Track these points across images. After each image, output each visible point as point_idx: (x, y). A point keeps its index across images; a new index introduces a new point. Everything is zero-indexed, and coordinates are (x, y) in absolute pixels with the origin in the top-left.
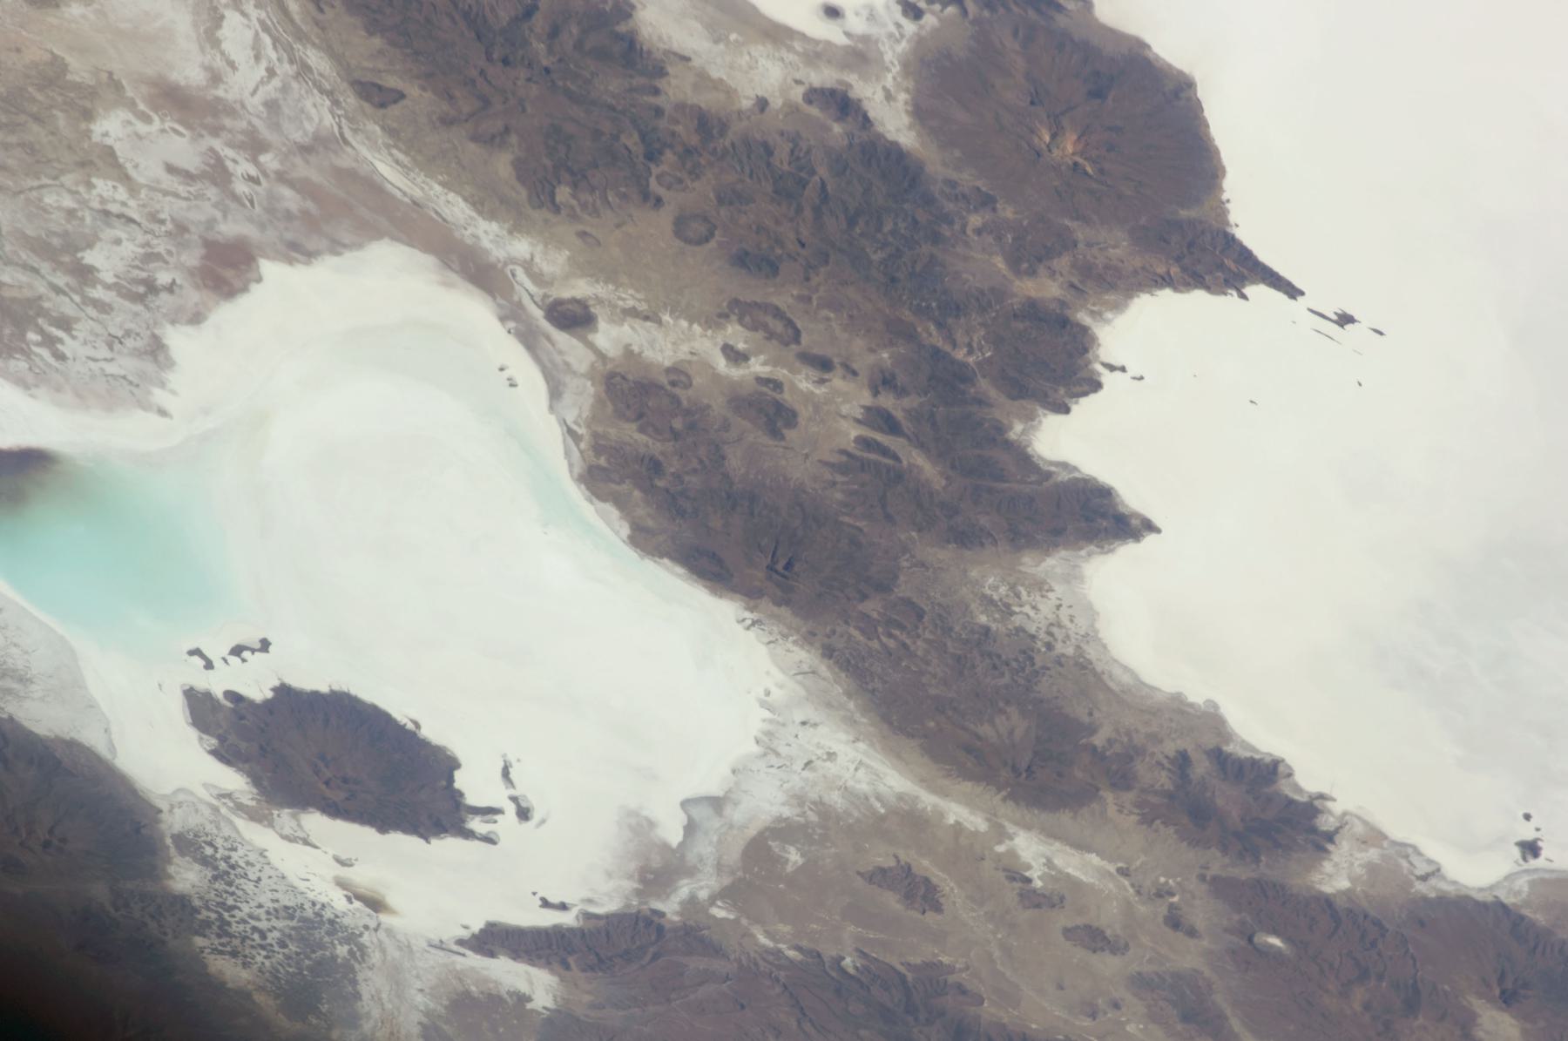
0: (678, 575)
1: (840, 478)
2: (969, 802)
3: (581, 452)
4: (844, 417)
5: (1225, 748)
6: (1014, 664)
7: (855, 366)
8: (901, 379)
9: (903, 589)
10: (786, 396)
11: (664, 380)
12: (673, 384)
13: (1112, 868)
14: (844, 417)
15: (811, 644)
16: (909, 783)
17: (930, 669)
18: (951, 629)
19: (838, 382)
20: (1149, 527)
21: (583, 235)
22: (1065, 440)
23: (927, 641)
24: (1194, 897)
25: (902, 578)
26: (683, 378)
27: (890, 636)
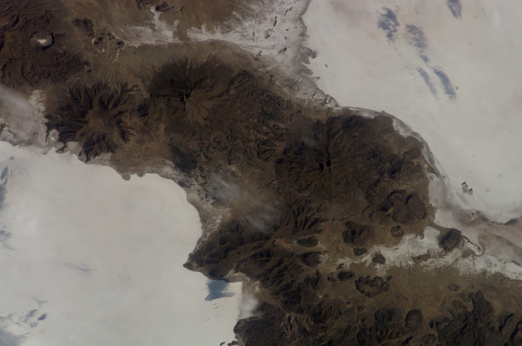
0: (365, 110)
1: (317, 216)
2: (200, 45)
3: (426, 162)
4: (326, 252)
5: (110, 154)
6: (212, 150)
7: (330, 283)
8: (310, 288)
9: (271, 165)
10: (351, 249)
11: (403, 227)
12: (398, 227)
13: (126, 42)
14: (326, 252)
15: (298, 105)
16: (228, 40)
17: (244, 124)
18: (244, 154)
19: (333, 269)
20: (188, 266)
21: (457, 288)
22: (239, 300)
23: (250, 141)
24: (86, 48)
25: (274, 173)
26: (396, 233)
27: (266, 134)
